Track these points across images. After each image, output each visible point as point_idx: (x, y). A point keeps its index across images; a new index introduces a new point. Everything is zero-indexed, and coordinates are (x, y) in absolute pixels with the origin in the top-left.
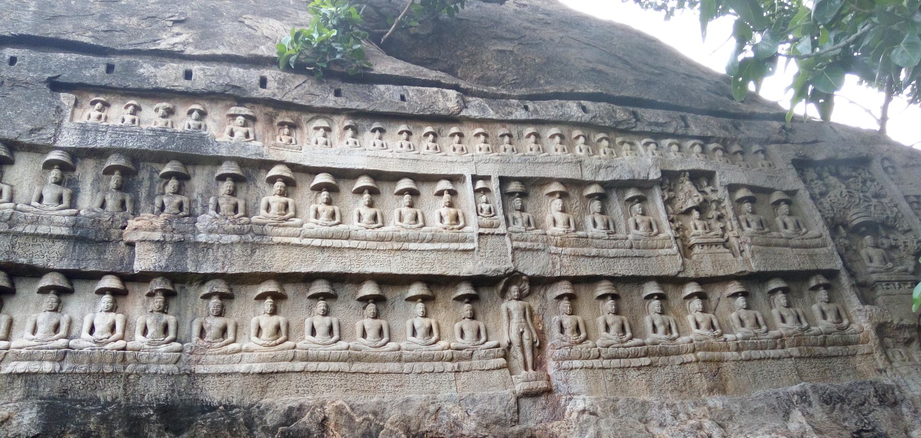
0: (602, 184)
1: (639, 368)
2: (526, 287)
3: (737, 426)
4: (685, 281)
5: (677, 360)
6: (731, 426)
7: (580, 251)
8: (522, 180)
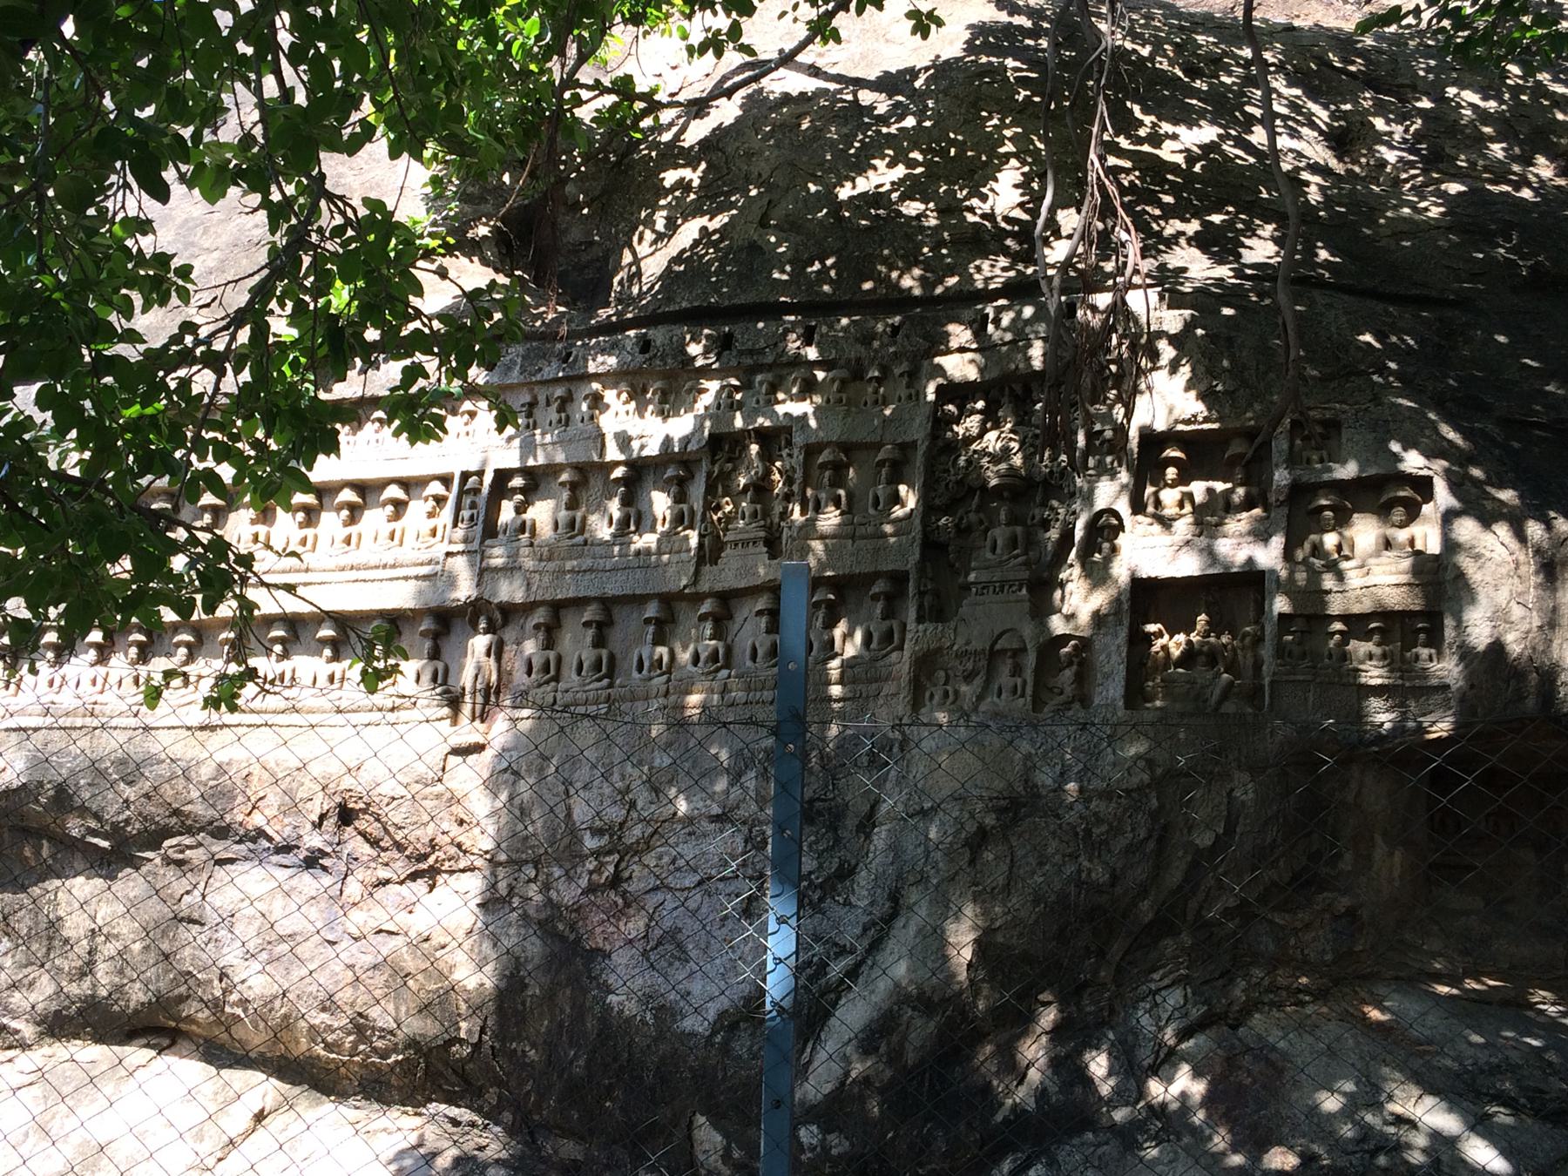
2: (498, 616)
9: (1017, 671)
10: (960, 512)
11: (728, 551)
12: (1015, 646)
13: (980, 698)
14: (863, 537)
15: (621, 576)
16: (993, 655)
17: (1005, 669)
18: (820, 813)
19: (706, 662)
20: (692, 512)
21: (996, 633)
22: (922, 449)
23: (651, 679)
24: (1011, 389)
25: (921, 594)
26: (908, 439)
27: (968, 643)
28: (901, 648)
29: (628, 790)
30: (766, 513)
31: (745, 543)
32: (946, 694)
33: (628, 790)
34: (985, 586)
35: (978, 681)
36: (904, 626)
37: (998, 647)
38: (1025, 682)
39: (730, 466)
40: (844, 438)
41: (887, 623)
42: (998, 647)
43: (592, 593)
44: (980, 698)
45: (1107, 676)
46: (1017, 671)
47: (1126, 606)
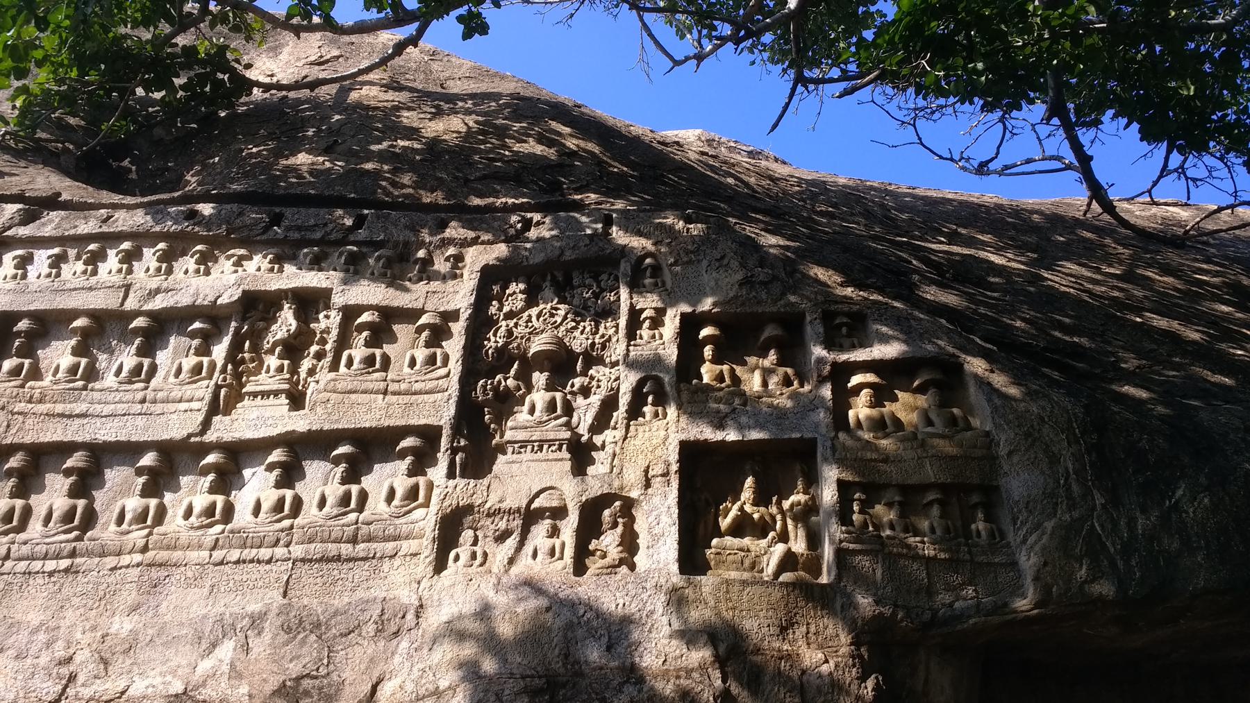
0: (150, 314)
1: (51, 574)
3: (128, 662)
4: (206, 449)
5: (110, 561)
6: (120, 661)
7: (59, 408)
8: (35, 316)
9: (554, 532)
10: (498, 377)
11: (246, 402)
12: (555, 504)
13: (511, 561)
14: (394, 393)
15: (117, 422)
16: (530, 517)
17: (540, 531)
18: (307, 693)
19: (200, 516)
20: (213, 365)
21: (534, 491)
22: (464, 315)
23: (128, 532)
24: (554, 279)
25: (454, 451)
26: (451, 307)
27: (500, 502)
28: (427, 504)
29: (69, 660)
30: (294, 370)
31: (265, 394)
32: (474, 556)
33: (69, 660)
34: (524, 444)
35: (512, 542)
36: (430, 486)
37: (536, 505)
38: (563, 545)
39: (261, 324)
40: (384, 303)
41: (414, 480)
42: (536, 505)
43: (79, 439)
44: (511, 561)
45: (656, 538)
46: (554, 532)
47: (675, 467)
